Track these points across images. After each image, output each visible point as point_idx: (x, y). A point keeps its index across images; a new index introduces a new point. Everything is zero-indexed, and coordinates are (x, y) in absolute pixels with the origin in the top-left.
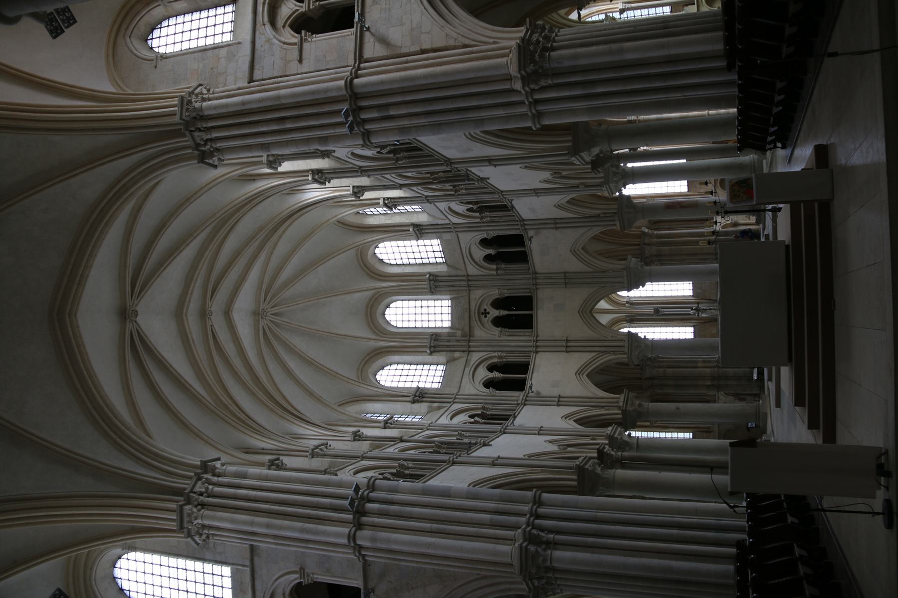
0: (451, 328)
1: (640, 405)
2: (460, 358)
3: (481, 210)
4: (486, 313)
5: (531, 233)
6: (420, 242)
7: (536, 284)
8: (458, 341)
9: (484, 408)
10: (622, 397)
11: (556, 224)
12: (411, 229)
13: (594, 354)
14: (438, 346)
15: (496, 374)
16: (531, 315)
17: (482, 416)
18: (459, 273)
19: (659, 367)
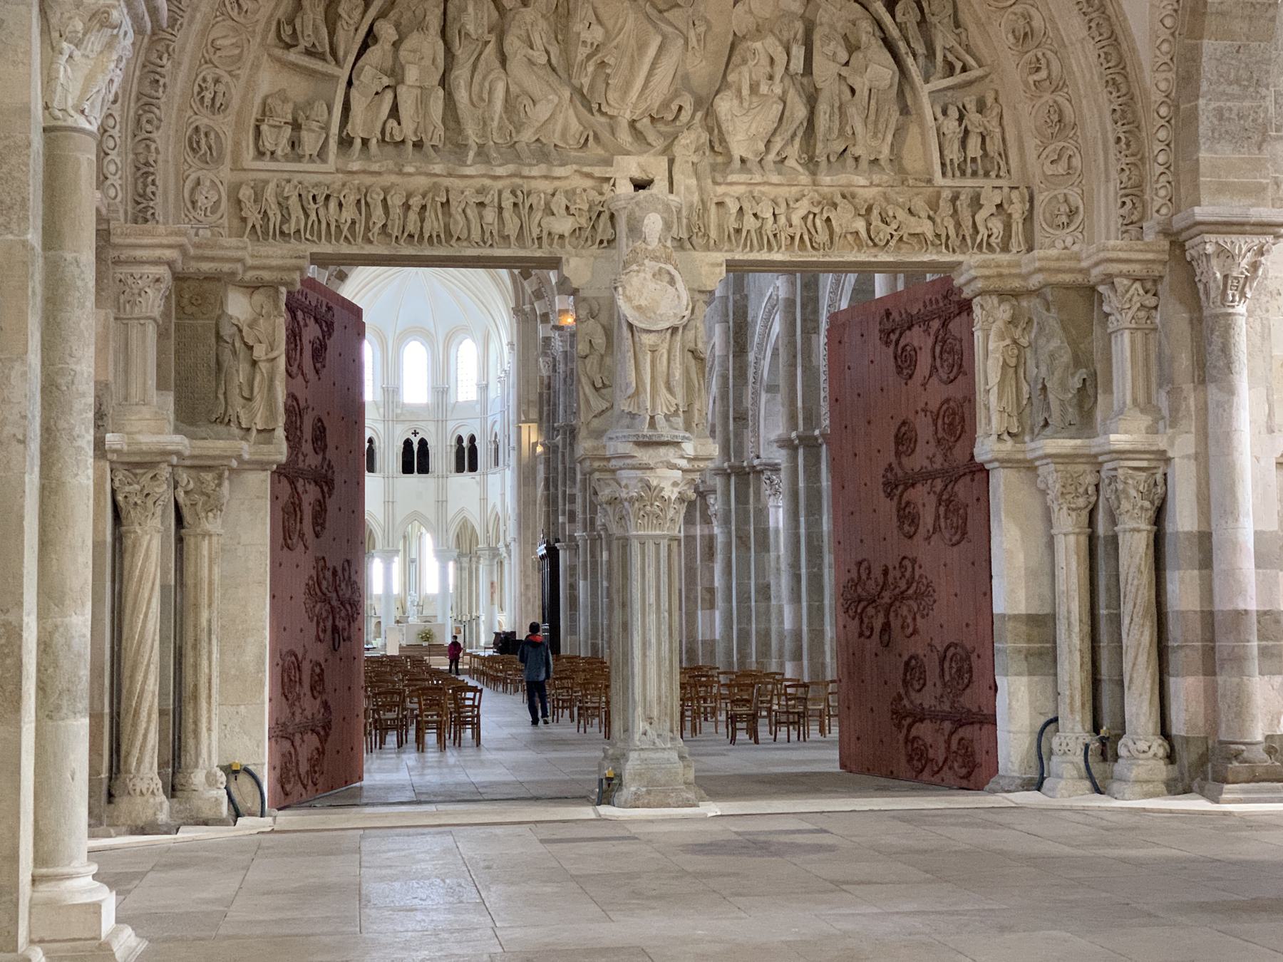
0: (403, 404)
3: (495, 441)
4: (415, 433)
5: (478, 478)
6: (475, 388)
11: (484, 500)
16: (412, 472)
18: (449, 414)
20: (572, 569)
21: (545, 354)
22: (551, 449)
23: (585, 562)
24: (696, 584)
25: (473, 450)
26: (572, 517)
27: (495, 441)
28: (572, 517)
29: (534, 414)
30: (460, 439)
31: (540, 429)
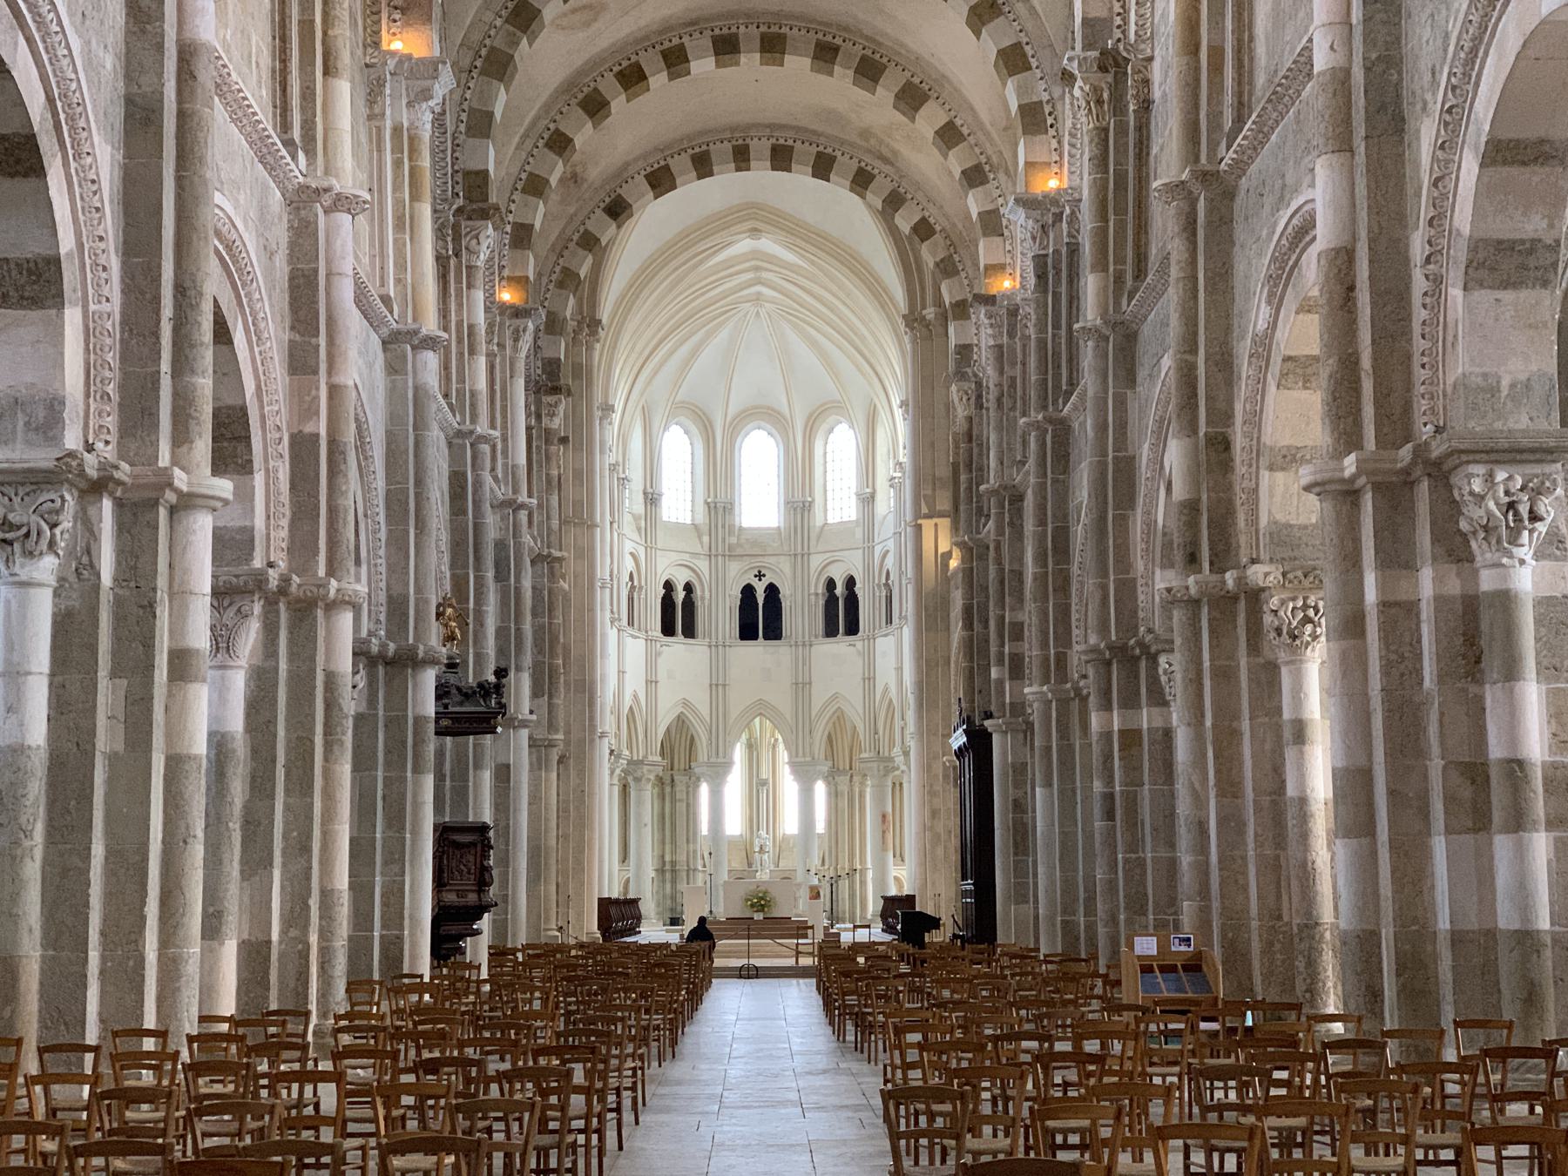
0: (741, 528)
1: (649, 780)
2: (701, 543)
3: (887, 585)
4: (760, 576)
5: (859, 645)
6: (854, 498)
7: (796, 645)
8: (724, 540)
9: (641, 588)
10: (660, 759)
11: (869, 679)
12: (868, 490)
13: (708, 719)
14: (716, 513)
15: (680, 596)
16: (755, 637)
17: (633, 587)
18: (813, 542)
19: (688, 793)
20: (1019, 771)
21: (961, 375)
22: (974, 553)
23: (1047, 749)
24: (1421, 753)
25: (852, 601)
26: (1017, 669)
27: (887, 585)
28: (1017, 669)
29: (944, 502)
30: (831, 584)
31: (955, 528)
